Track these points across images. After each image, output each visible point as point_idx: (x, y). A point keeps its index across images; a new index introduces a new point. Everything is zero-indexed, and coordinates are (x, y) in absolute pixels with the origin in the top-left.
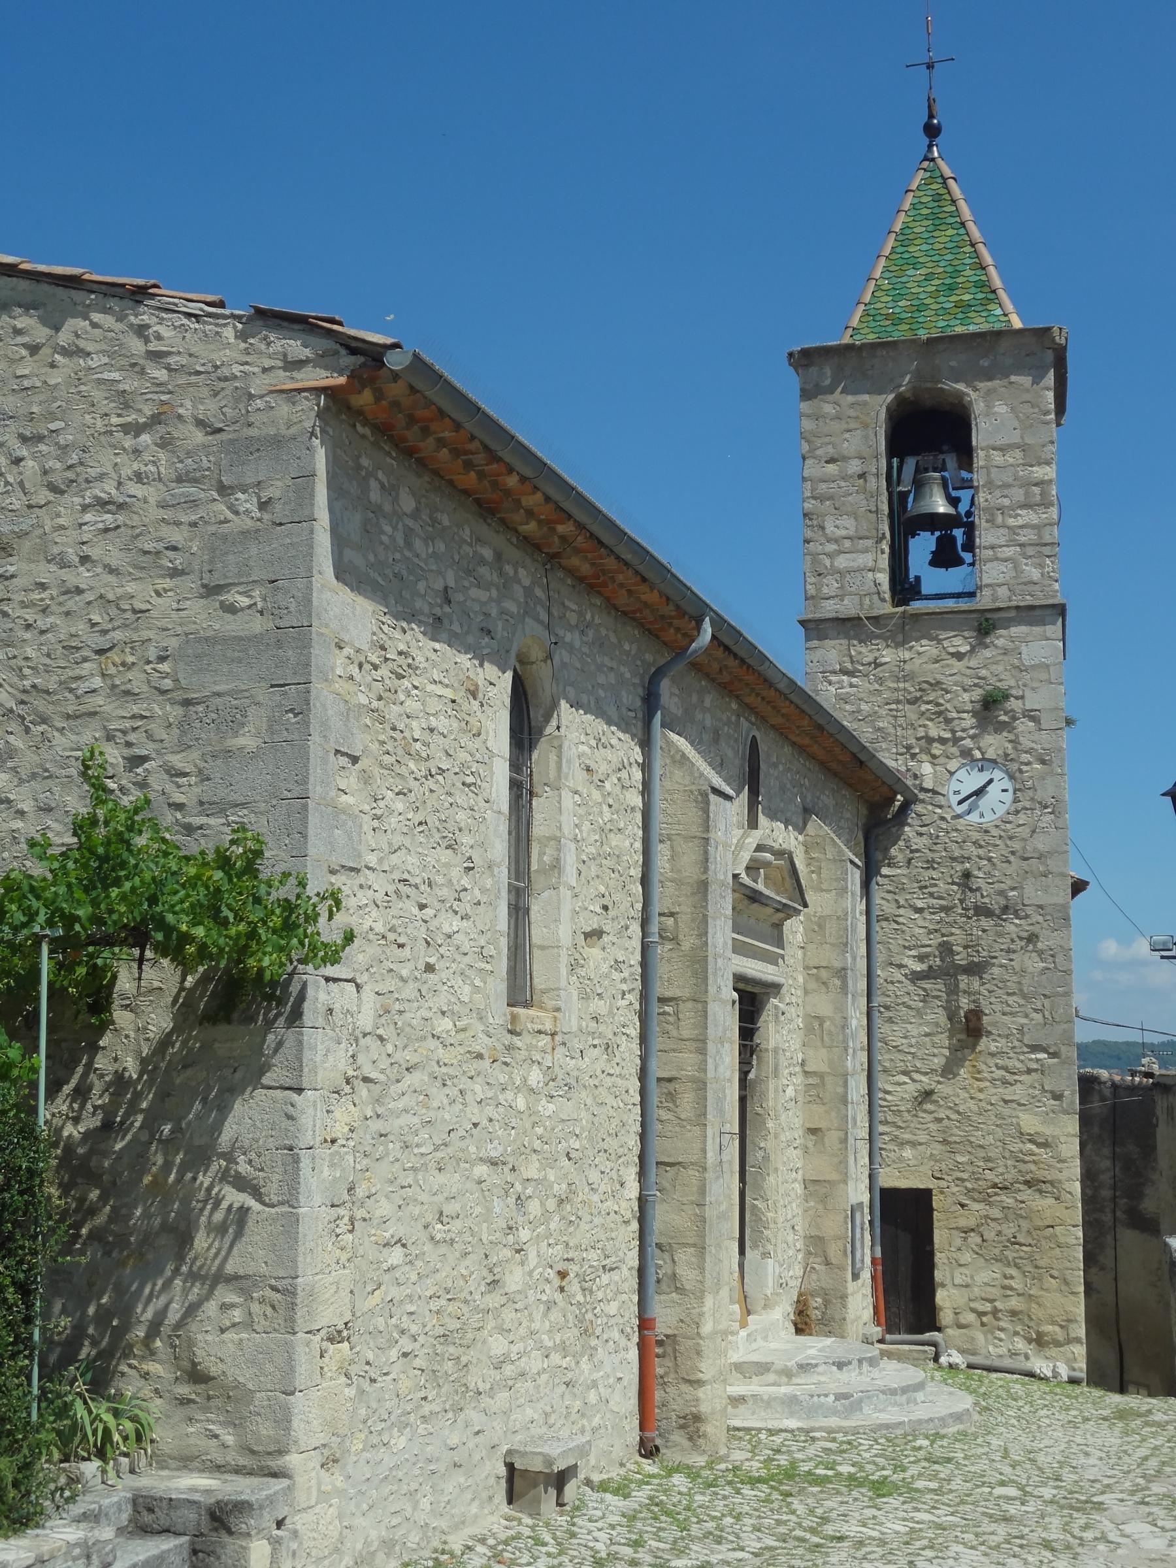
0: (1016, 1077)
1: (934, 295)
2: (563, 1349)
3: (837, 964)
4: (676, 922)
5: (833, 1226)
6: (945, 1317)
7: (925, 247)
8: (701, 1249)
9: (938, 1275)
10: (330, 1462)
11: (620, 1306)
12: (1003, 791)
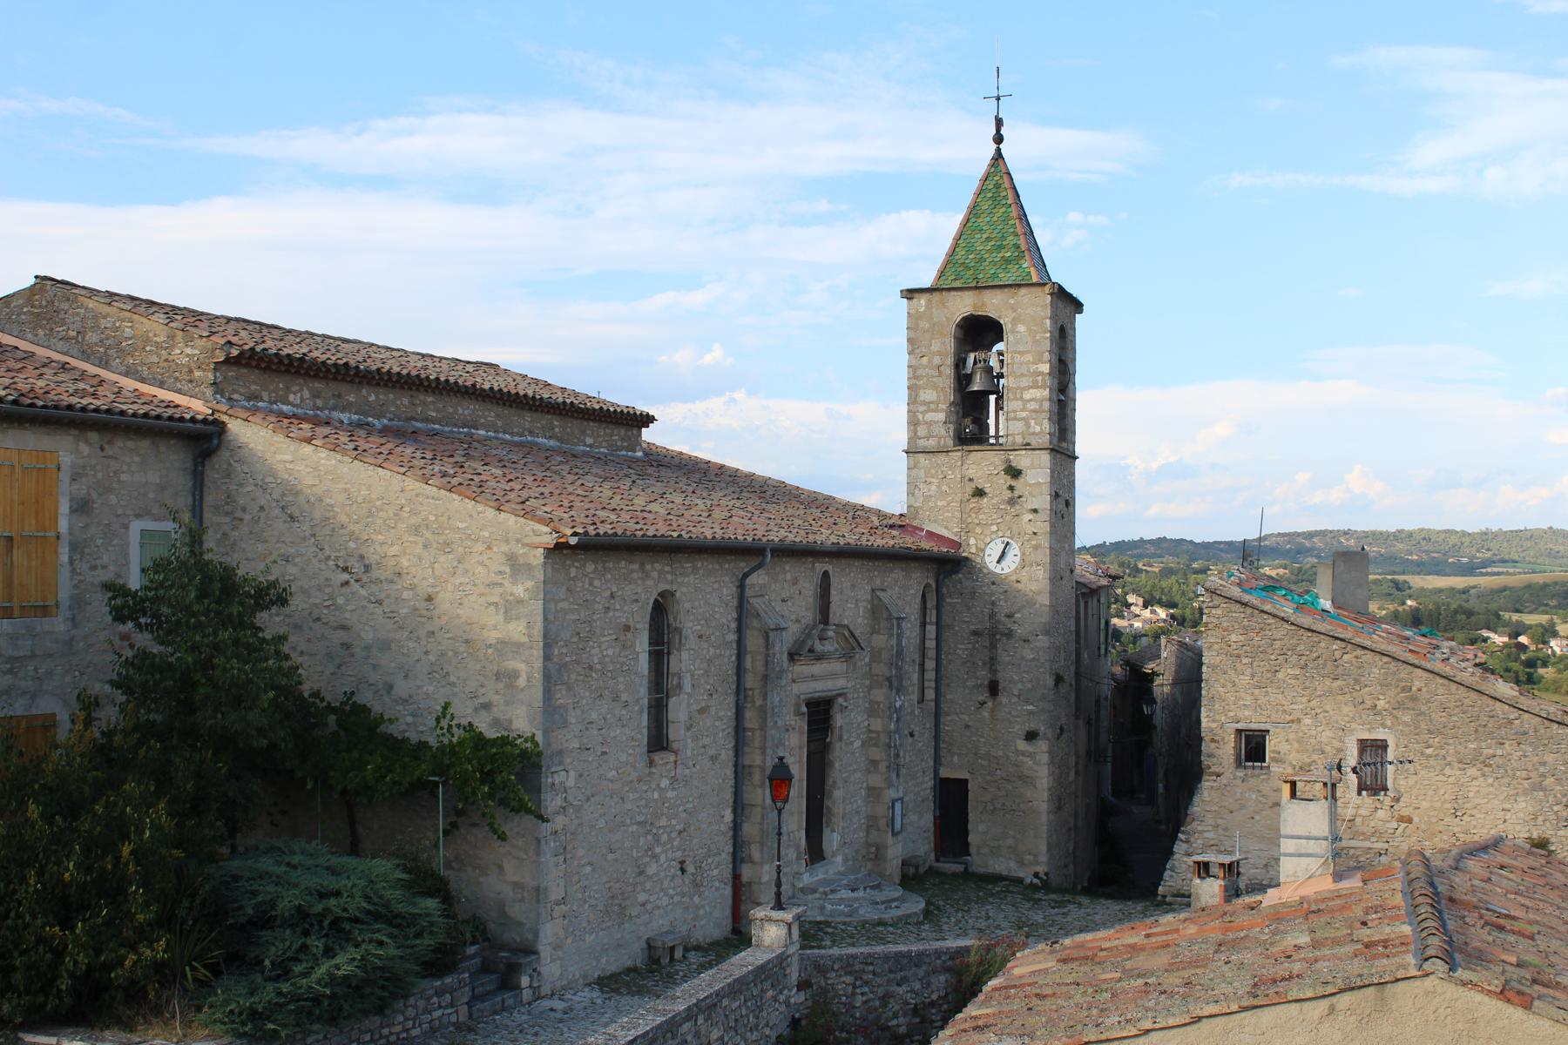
3: (887, 674)
6: (973, 850)
9: (970, 826)
10: (557, 947)
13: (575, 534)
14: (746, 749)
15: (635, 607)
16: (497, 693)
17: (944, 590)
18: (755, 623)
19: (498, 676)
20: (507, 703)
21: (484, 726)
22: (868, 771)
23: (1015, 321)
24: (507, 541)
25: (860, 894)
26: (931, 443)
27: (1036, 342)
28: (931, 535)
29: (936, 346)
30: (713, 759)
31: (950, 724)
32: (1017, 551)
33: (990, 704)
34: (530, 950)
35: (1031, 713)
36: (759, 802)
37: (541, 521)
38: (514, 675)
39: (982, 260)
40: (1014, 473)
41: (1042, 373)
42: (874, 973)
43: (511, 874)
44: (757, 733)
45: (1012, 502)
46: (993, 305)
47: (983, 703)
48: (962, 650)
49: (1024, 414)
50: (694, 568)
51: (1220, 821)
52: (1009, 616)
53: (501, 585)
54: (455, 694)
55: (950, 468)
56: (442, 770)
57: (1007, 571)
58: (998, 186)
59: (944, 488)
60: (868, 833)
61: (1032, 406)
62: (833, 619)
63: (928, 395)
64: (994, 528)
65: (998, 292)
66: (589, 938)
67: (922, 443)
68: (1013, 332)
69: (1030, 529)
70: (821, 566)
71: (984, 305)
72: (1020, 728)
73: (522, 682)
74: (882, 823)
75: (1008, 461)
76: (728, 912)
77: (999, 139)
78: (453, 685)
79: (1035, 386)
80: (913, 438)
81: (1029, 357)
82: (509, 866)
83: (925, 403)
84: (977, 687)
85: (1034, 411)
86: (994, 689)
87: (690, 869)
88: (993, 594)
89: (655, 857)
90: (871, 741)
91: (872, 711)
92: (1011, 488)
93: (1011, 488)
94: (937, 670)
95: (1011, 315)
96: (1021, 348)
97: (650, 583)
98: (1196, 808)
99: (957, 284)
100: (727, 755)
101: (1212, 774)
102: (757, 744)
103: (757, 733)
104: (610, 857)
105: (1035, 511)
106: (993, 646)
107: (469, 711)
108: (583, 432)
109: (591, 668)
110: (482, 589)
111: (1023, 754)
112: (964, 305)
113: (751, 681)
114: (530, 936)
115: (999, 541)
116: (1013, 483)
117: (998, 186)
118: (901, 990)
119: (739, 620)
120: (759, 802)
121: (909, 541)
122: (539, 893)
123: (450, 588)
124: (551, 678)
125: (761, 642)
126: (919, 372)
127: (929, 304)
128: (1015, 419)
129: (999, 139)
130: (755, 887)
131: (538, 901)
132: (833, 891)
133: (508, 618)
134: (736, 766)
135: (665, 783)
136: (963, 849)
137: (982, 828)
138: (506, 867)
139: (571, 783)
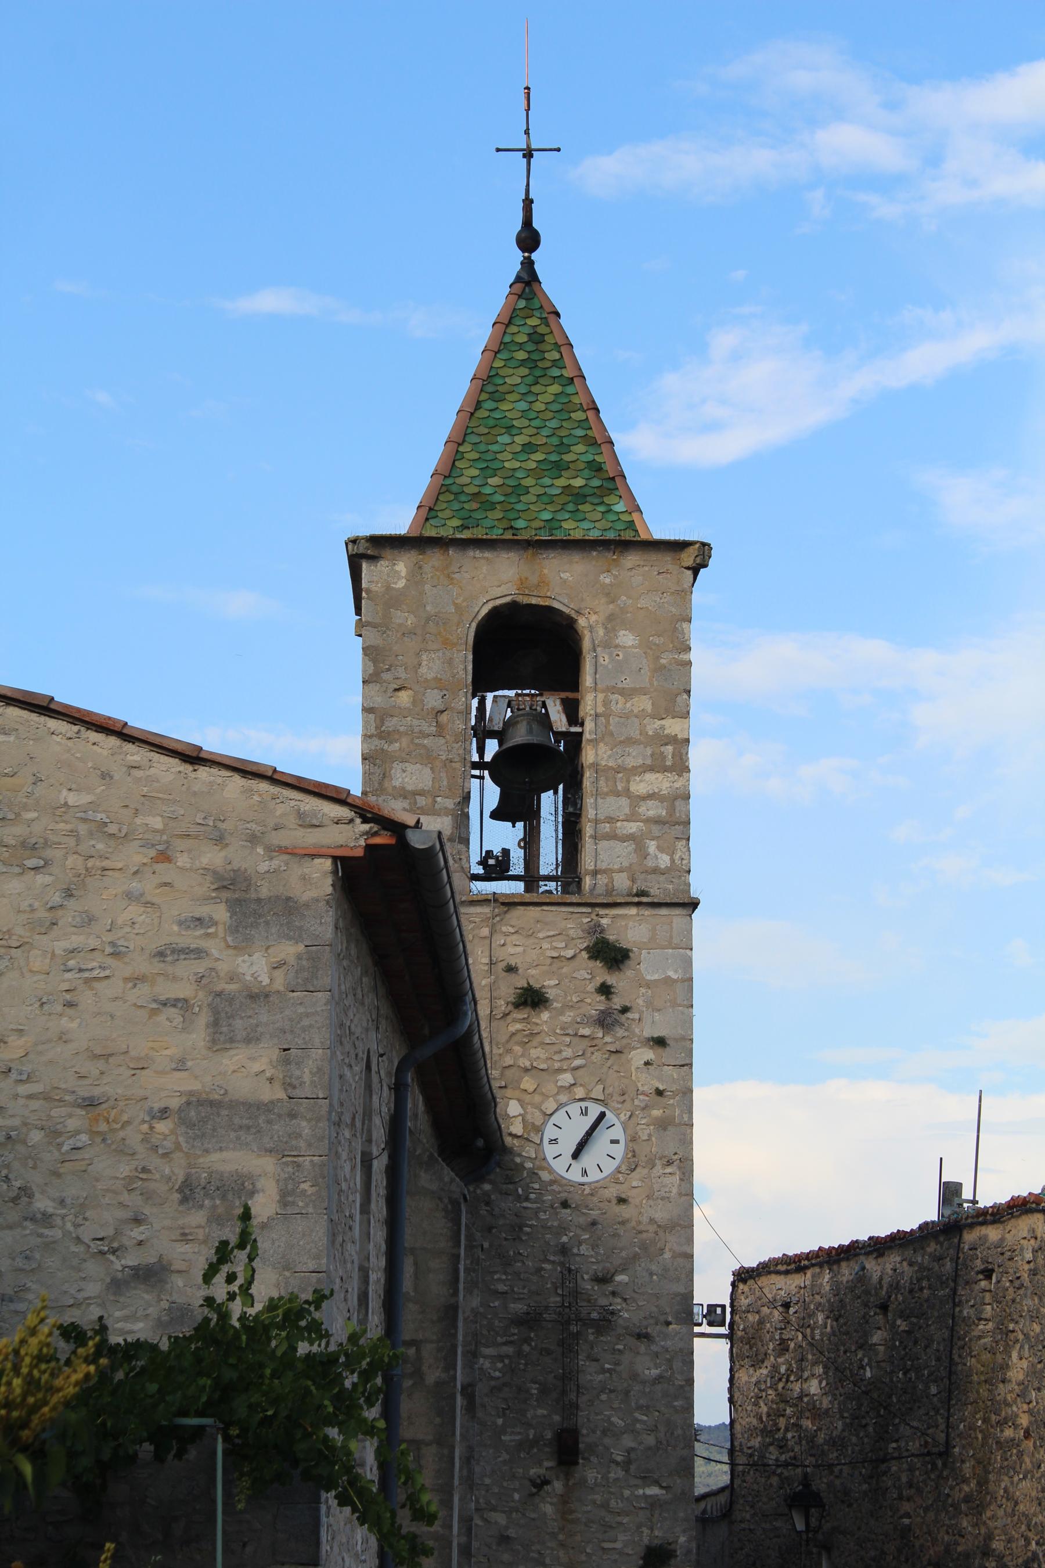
0: (619, 1519)
4: (418, 1350)
7: (523, 405)
12: (613, 1142)
16: (185, 1237)
21: (136, 1321)
23: (612, 622)
24: (220, 840)
29: (431, 666)
32: (617, 1132)
33: (558, 1486)
35: (653, 1504)
39: (519, 490)
44: (430, 1453)
45: (605, 1021)
47: (541, 1484)
49: (632, 827)
52: (603, 1280)
53: (199, 953)
54: (49, 1246)
57: (594, 1176)
58: (537, 338)
64: (567, 1078)
68: (608, 645)
71: (543, 582)
75: (596, 929)
78: (46, 1219)
81: (644, 703)
85: (658, 821)
86: (567, 1450)
88: (563, 1229)
92: (605, 990)
93: (605, 990)
95: (604, 608)
96: (628, 683)
103: (430, 1453)
105: (660, 1042)
106: (568, 1345)
107: (93, 1289)
110: (143, 965)
112: (495, 580)
117: (537, 338)
123: (38, 962)
126: (391, 724)
127: (416, 572)
128: (613, 836)
133: (222, 1035)
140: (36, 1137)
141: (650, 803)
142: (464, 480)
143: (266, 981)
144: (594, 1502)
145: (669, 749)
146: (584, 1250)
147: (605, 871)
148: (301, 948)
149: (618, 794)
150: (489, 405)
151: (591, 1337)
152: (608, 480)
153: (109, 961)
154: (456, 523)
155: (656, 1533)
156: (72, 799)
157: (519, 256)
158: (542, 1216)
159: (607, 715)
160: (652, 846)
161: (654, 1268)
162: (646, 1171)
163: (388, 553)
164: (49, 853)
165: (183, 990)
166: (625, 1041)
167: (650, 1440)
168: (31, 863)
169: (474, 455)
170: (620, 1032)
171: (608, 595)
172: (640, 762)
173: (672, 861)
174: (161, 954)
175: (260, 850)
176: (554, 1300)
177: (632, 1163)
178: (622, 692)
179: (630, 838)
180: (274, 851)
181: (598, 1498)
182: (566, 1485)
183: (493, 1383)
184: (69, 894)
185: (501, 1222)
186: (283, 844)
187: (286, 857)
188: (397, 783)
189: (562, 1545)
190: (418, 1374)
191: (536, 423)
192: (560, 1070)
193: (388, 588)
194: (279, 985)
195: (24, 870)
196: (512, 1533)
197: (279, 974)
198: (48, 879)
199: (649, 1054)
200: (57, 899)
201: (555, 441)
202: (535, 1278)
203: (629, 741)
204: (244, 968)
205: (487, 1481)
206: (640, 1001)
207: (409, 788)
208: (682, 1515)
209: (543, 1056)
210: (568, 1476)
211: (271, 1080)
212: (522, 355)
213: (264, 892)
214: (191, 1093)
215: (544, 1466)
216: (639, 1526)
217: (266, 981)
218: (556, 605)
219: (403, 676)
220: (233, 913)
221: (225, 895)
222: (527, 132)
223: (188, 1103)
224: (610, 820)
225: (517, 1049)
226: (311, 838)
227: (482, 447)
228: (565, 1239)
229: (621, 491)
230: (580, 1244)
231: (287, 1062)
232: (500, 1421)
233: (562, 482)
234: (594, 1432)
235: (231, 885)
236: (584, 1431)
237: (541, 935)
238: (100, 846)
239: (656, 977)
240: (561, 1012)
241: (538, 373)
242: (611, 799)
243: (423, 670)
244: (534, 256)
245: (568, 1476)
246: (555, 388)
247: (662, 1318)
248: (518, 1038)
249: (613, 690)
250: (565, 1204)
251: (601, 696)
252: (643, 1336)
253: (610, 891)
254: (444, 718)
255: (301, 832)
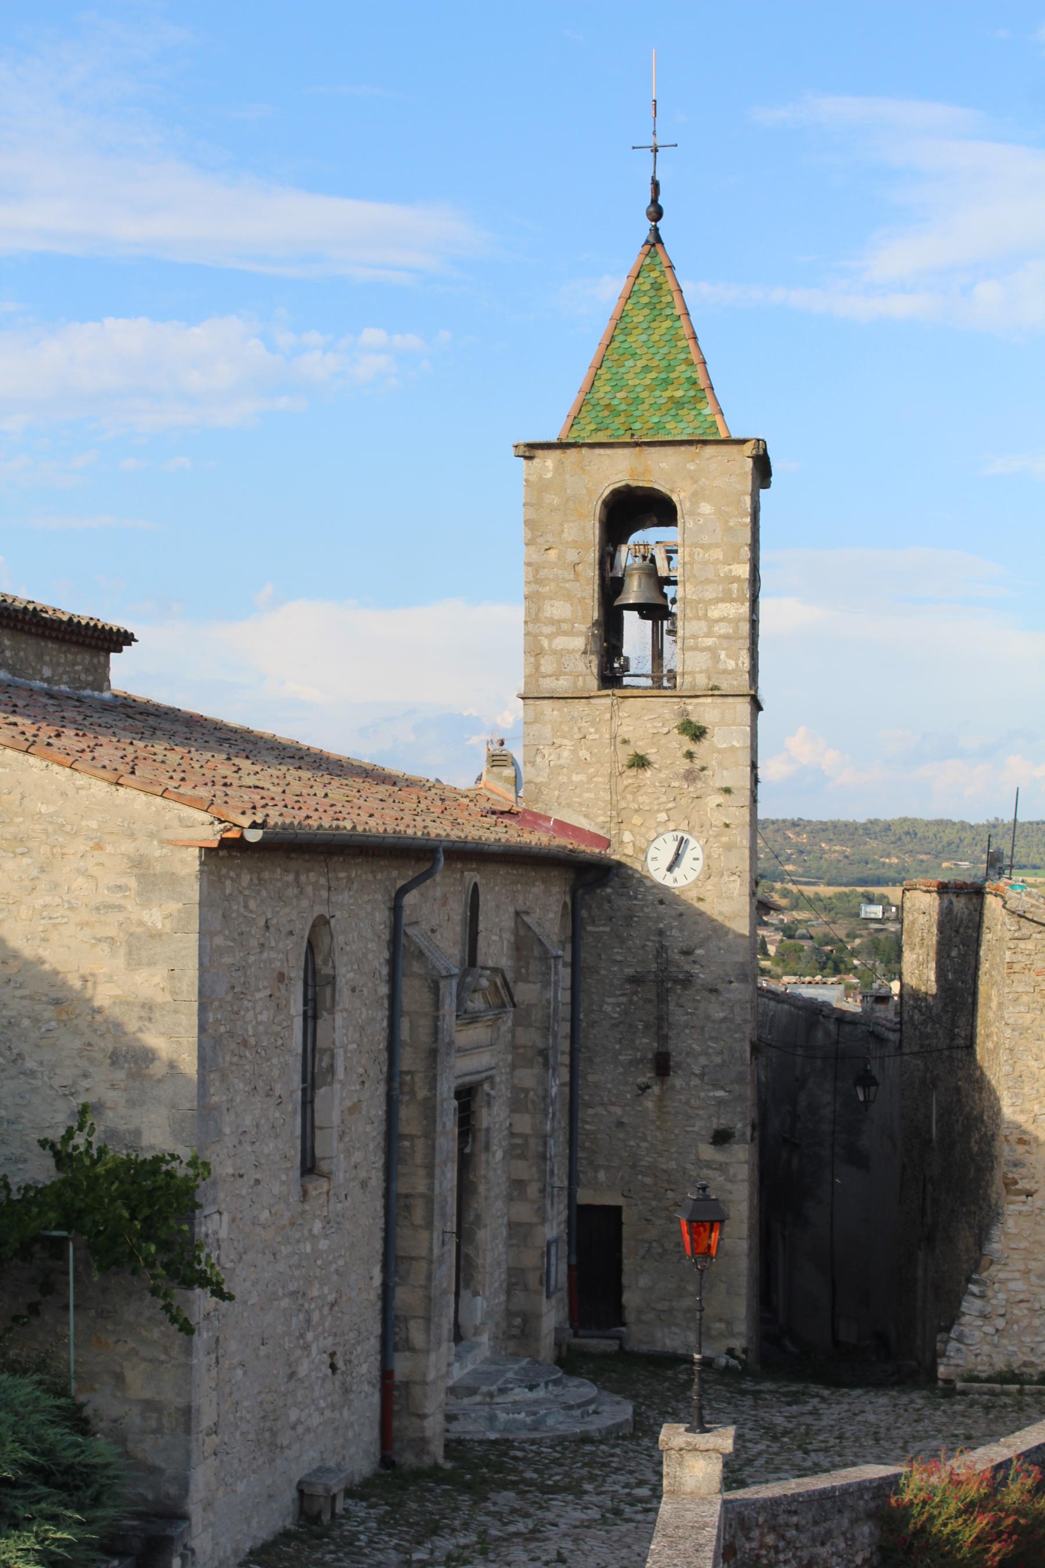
0: (696, 1112)
1: (650, 388)
2: (333, 1407)
3: (540, 1045)
4: (413, 1078)
5: (531, 1258)
6: (630, 1316)
7: (644, 337)
8: (428, 1320)
9: (625, 1280)
11: (368, 1368)
12: (695, 859)
13: (254, 825)
14: (401, 1169)
15: (290, 943)
17: (584, 913)
18: (416, 967)
19: (115, 1059)
20: (132, 1103)
22: (510, 1198)
23: (696, 497)
24: (132, 836)
25: (540, 1393)
26: (562, 685)
27: (728, 530)
28: (562, 827)
29: (570, 532)
30: (364, 1184)
31: (591, 1120)
32: (698, 853)
33: (656, 1089)
34: (177, 1515)
35: (720, 1102)
36: (424, 1253)
37: (193, 803)
38: (148, 1056)
39: (637, 401)
40: (697, 733)
41: (737, 579)
42: (797, 1527)
43: (139, 1383)
44: (420, 1144)
45: (690, 777)
46: (659, 471)
48: (611, 1006)
49: (709, 642)
50: (350, 881)
51: (1032, 1265)
52: (687, 953)
53: (120, 908)
54: (34, 1090)
55: (593, 723)
56: (71, 1219)
57: (682, 883)
58: (657, 286)
59: (583, 754)
60: (509, 1293)
61: (722, 629)
62: (481, 959)
63: (557, 609)
65: (670, 450)
66: (240, 1487)
67: (548, 685)
69: (719, 819)
70: (472, 876)
72: (703, 1125)
73: (158, 1069)
74: (533, 1279)
75: (684, 713)
76: (376, 1432)
77: (656, 213)
78: (32, 1074)
79: (727, 598)
80: (534, 675)
81: (718, 554)
82: (135, 1375)
83: (552, 622)
84: (634, 1063)
85: (727, 637)
86: (662, 1066)
87: (340, 1364)
88: (660, 919)
89: (307, 1347)
90: (516, 1151)
91: (516, 1105)
92: (690, 755)
93: (690, 755)
94: (573, 1037)
96: (705, 539)
97: (305, 903)
98: (996, 1246)
99: (601, 437)
100: (377, 1179)
101: (1019, 1192)
102: (419, 1159)
104: (263, 1351)
105: (728, 791)
106: (662, 998)
108: (40, 657)
109: (245, 1043)
111: (708, 1164)
112: (617, 470)
113: (408, 1060)
114: (173, 1490)
115: (669, 837)
116: (693, 747)
117: (657, 286)
118: (824, 1551)
119: (393, 963)
120: (424, 1253)
121: (537, 839)
122: (187, 1413)
124: (202, 1059)
125: (426, 997)
126: (543, 573)
128: (696, 648)
129: (656, 213)
130: (416, 1390)
131: (188, 1431)
132: (502, 1391)
133: (134, 962)
134: (387, 1194)
135: (317, 1226)
136: (615, 1314)
137: (643, 1281)
138: (130, 1375)
139: (223, 1234)
140: (26, 1022)
141: (721, 624)
142: (601, 395)
143: (160, 927)
144: (680, 1100)
145: (735, 585)
146: (675, 932)
147: (689, 673)
148: (180, 905)
149: (699, 619)
150: (621, 338)
151: (679, 991)
152: (702, 391)
153: (67, 913)
154: (593, 427)
155: (722, 1121)
156: (44, 809)
157: (650, 224)
158: (646, 910)
159: (692, 564)
160: (723, 655)
161: (721, 945)
162: (716, 879)
163: (539, 453)
164: (30, 844)
165: (112, 931)
166: (702, 791)
167: (718, 1060)
168: (20, 850)
169: (609, 376)
170: (699, 784)
171: (692, 478)
172: (714, 595)
173: (737, 664)
174: (98, 909)
175: (155, 843)
176: (654, 967)
177: (708, 873)
178: (702, 546)
179: (708, 649)
180: (164, 842)
181: (683, 1098)
182: (662, 1089)
183: (613, 1021)
184: (42, 870)
185: (618, 914)
186: (171, 838)
187: (171, 847)
188: (548, 615)
189: (659, 1128)
190: (413, 1093)
191: (652, 350)
192: (659, 811)
193: (541, 478)
194: (168, 929)
195: (15, 855)
196: (625, 1120)
197: (168, 922)
198: (29, 861)
199: (720, 799)
200: (35, 873)
201: (664, 363)
202: (641, 952)
203: (708, 581)
204: (146, 918)
205: (609, 1086)
206: (714, 763)
207: (556, 618)
208: (739, 1109)
209: (647, 801)
210: (663, 1083)
211: (163, 989)
212: (645, 300)
213: (158, 869)
214: (116, 996)
215: (647, 1076)
216: (710, 1117)
217: (160, 927)
218: (656, 486)
219: (551, 539)
220: (140, 883)
221: (135, 871)
222: (654, 134)
223: (114, 1003)
224: (695, 637)
225: (629, 797)
226: (185, 834)
227: (614, 370)
228: (661, 925)
229: (709, 399)
230: (672, 929)
231: (172, 978)
232: (618, 1047)
233: (668, 394)
234: (680, 1054)
235: (139, 864)
236: (674, 1054)
237: (646, 718)
238: (61, 839)
239: (725, 746)
240: (659, 770)
241: (656, 312)
242: (694, 623)
243: (565, 535)
244: (659, 224)
245: (663, 1083)
246: (668, 323)
247: (727, 979)
248: (630, 789)
249: (696, 545)
250: (661, 902)
251: (687, 550)
252: (714, 991)
253: (693, 687)
254: (579, 568)
255: (181, 830)
